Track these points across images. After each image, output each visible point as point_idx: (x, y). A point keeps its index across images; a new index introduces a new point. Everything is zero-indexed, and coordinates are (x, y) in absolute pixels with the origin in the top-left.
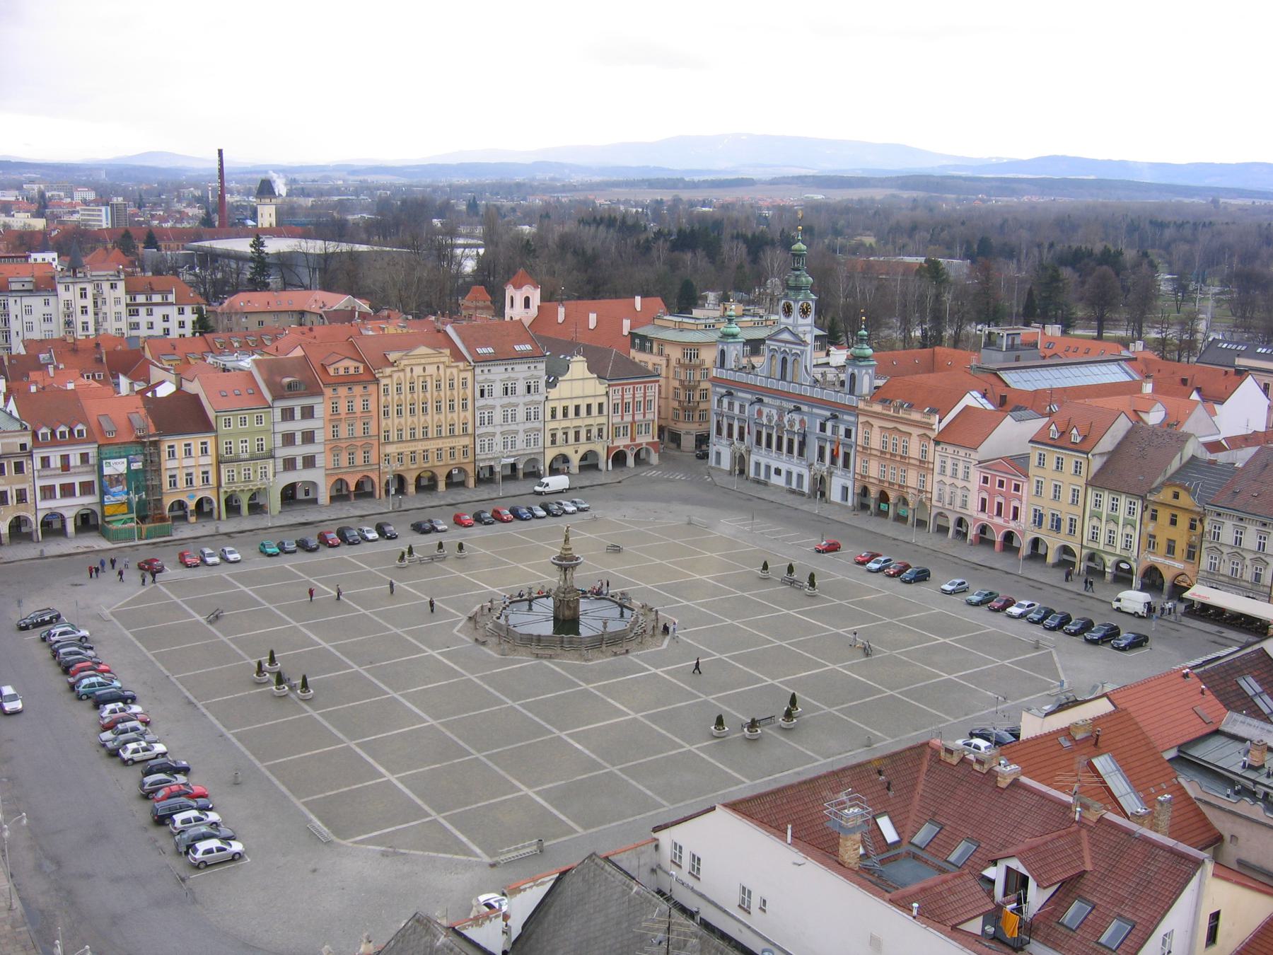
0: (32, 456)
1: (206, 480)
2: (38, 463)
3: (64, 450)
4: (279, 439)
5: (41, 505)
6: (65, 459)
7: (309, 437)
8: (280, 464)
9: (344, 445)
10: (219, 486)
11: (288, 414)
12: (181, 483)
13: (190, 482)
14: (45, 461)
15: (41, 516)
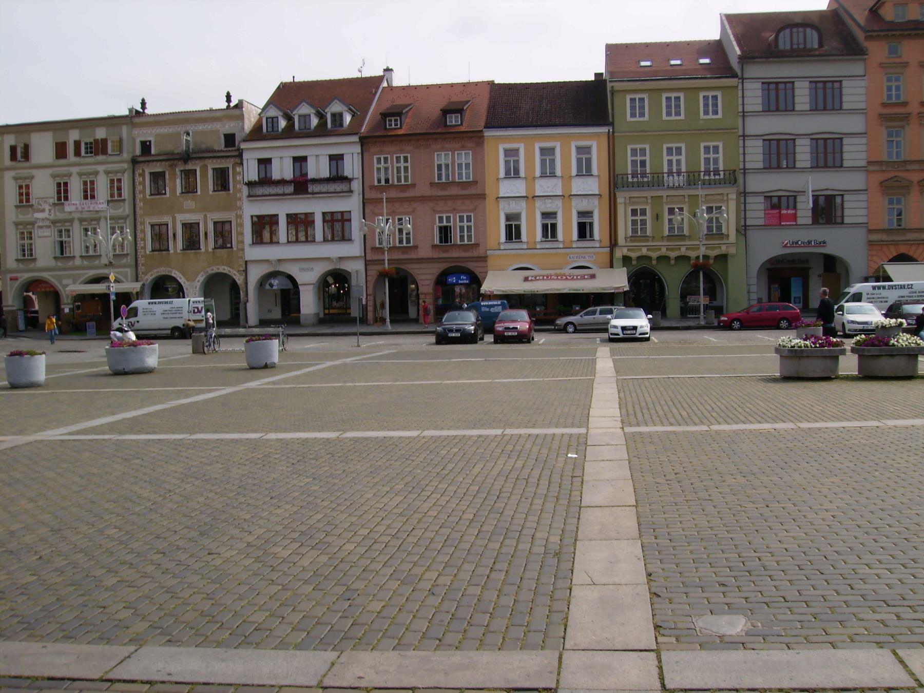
0: (240, 156)
1: (584, 231)
2: (251, 172)
3: (298, 146)
4: (755, 154)
5: (254, 253)
6: (300, 161)
7: (828, 153)
8: (757, 210)
9: (916, 177)
10: (613, 244)
11: (778, 98)
12: (531, 229)
13: (549, 231)
14: (265, 163)
15: (255, 274)
